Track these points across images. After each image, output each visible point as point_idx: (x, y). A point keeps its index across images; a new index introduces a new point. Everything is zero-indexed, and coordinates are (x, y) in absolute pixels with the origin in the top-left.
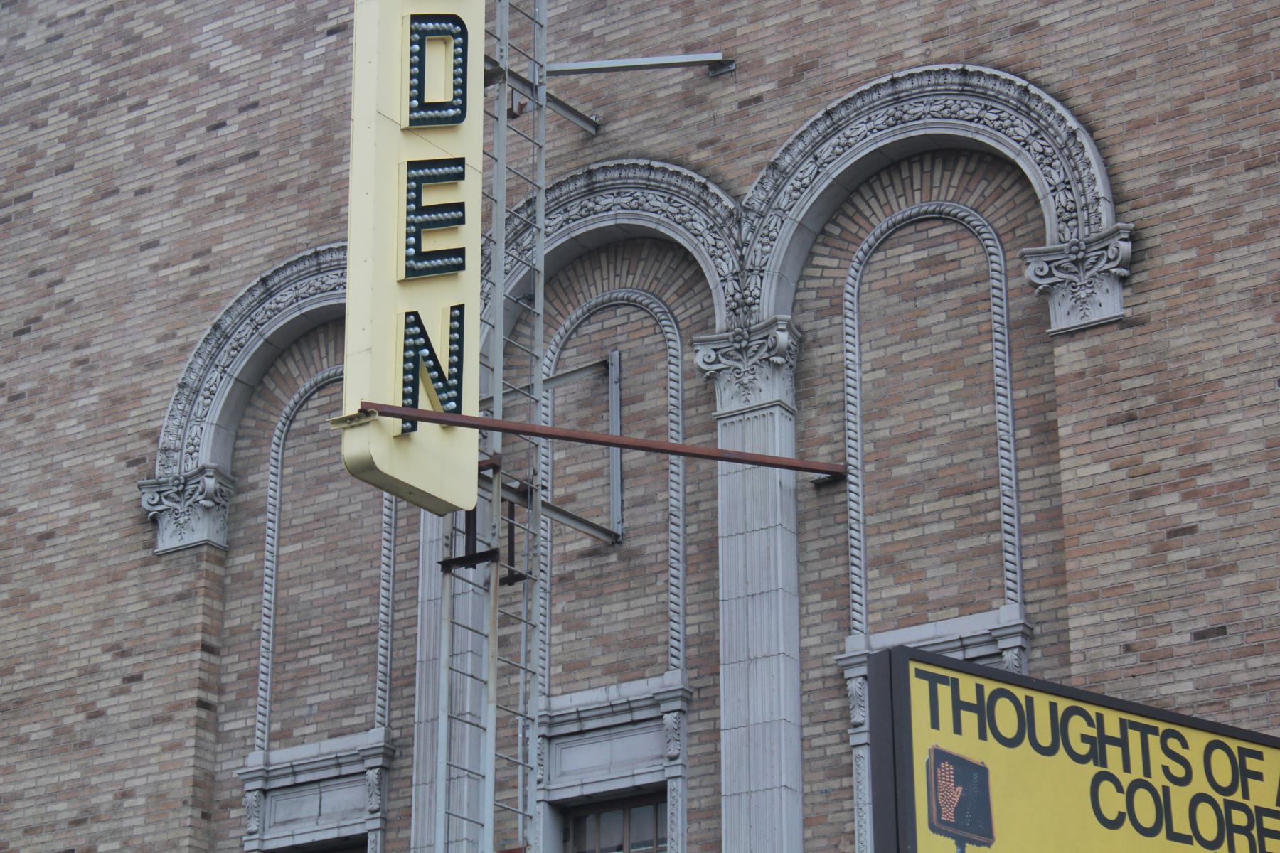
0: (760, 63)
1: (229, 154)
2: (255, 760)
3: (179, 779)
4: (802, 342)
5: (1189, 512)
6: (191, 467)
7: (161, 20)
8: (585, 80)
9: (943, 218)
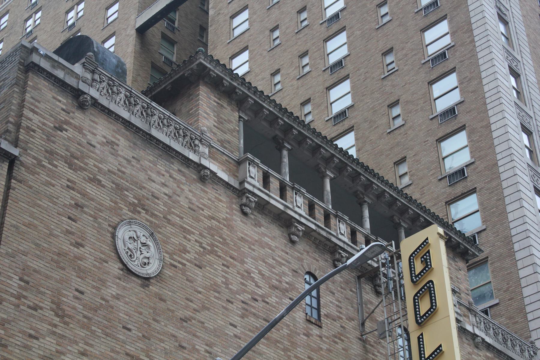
1: (260, 314)
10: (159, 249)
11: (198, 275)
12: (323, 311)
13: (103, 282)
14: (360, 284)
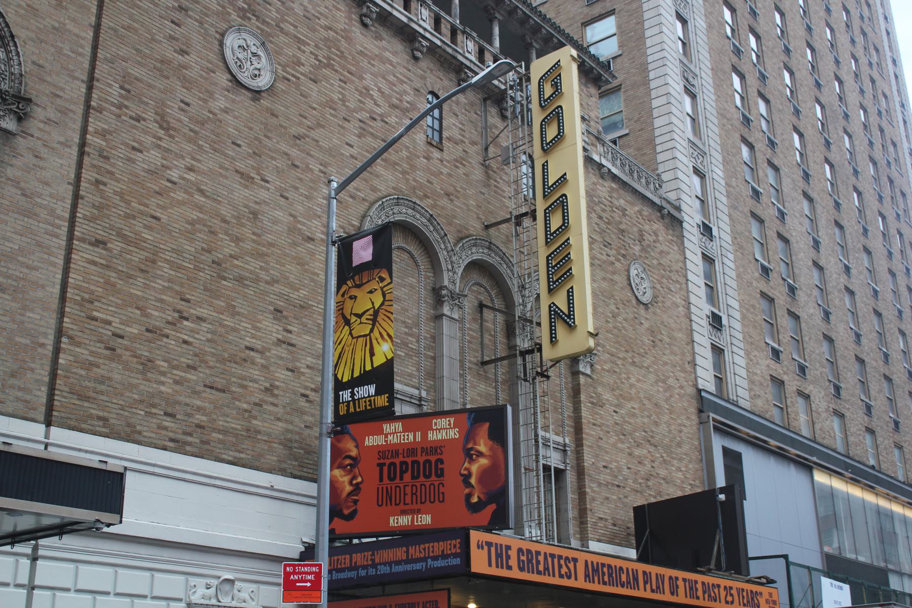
5: (602, 435)
10: (270, 60)
11: (313, 90)
12: (445, 134)
13: (211, 94)
14: (485, 107)
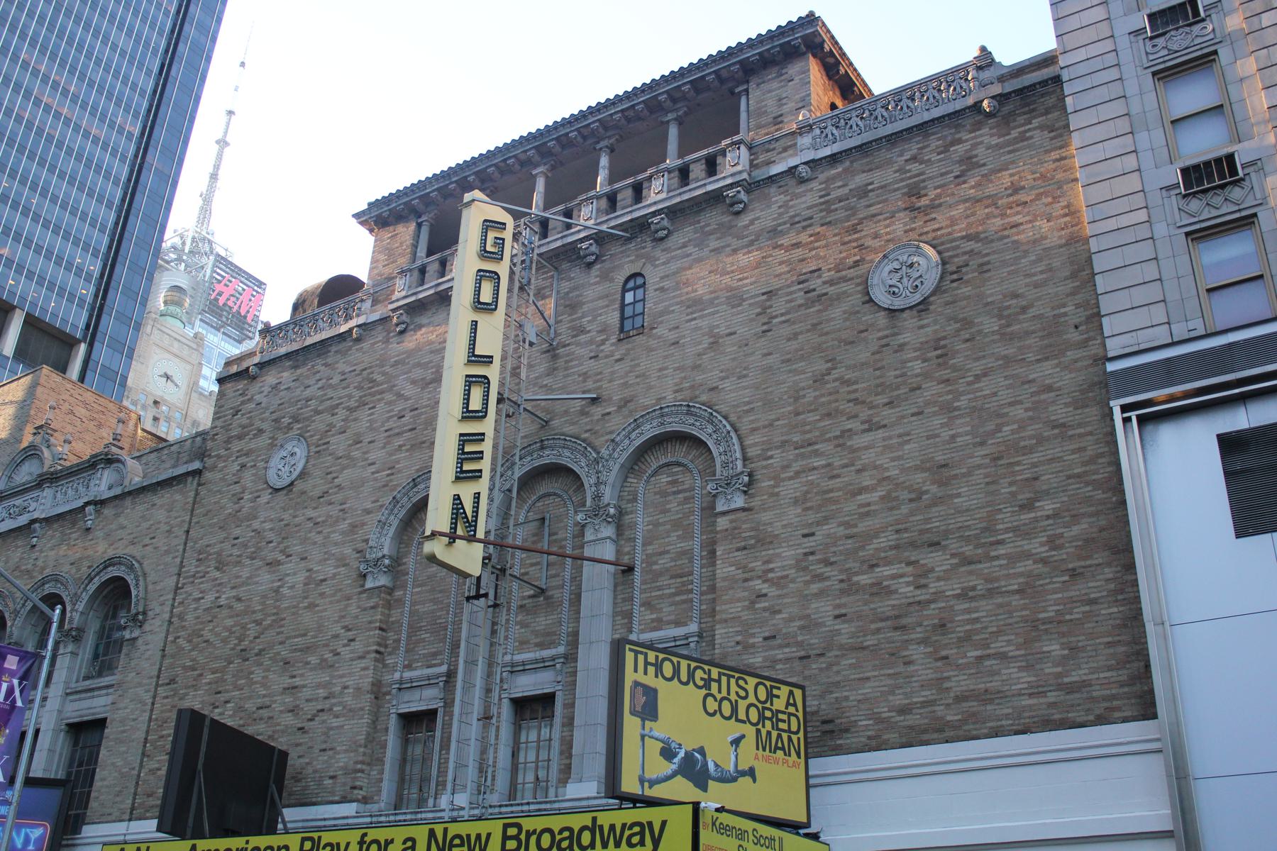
0: (610, 399)
2: (397, 676)
3: (366, 682)
4: (621, 513)
5: (765, 588)
6: (380, 555)
7: (384, 374)
8: (543, 403)
9: (678, 464)
